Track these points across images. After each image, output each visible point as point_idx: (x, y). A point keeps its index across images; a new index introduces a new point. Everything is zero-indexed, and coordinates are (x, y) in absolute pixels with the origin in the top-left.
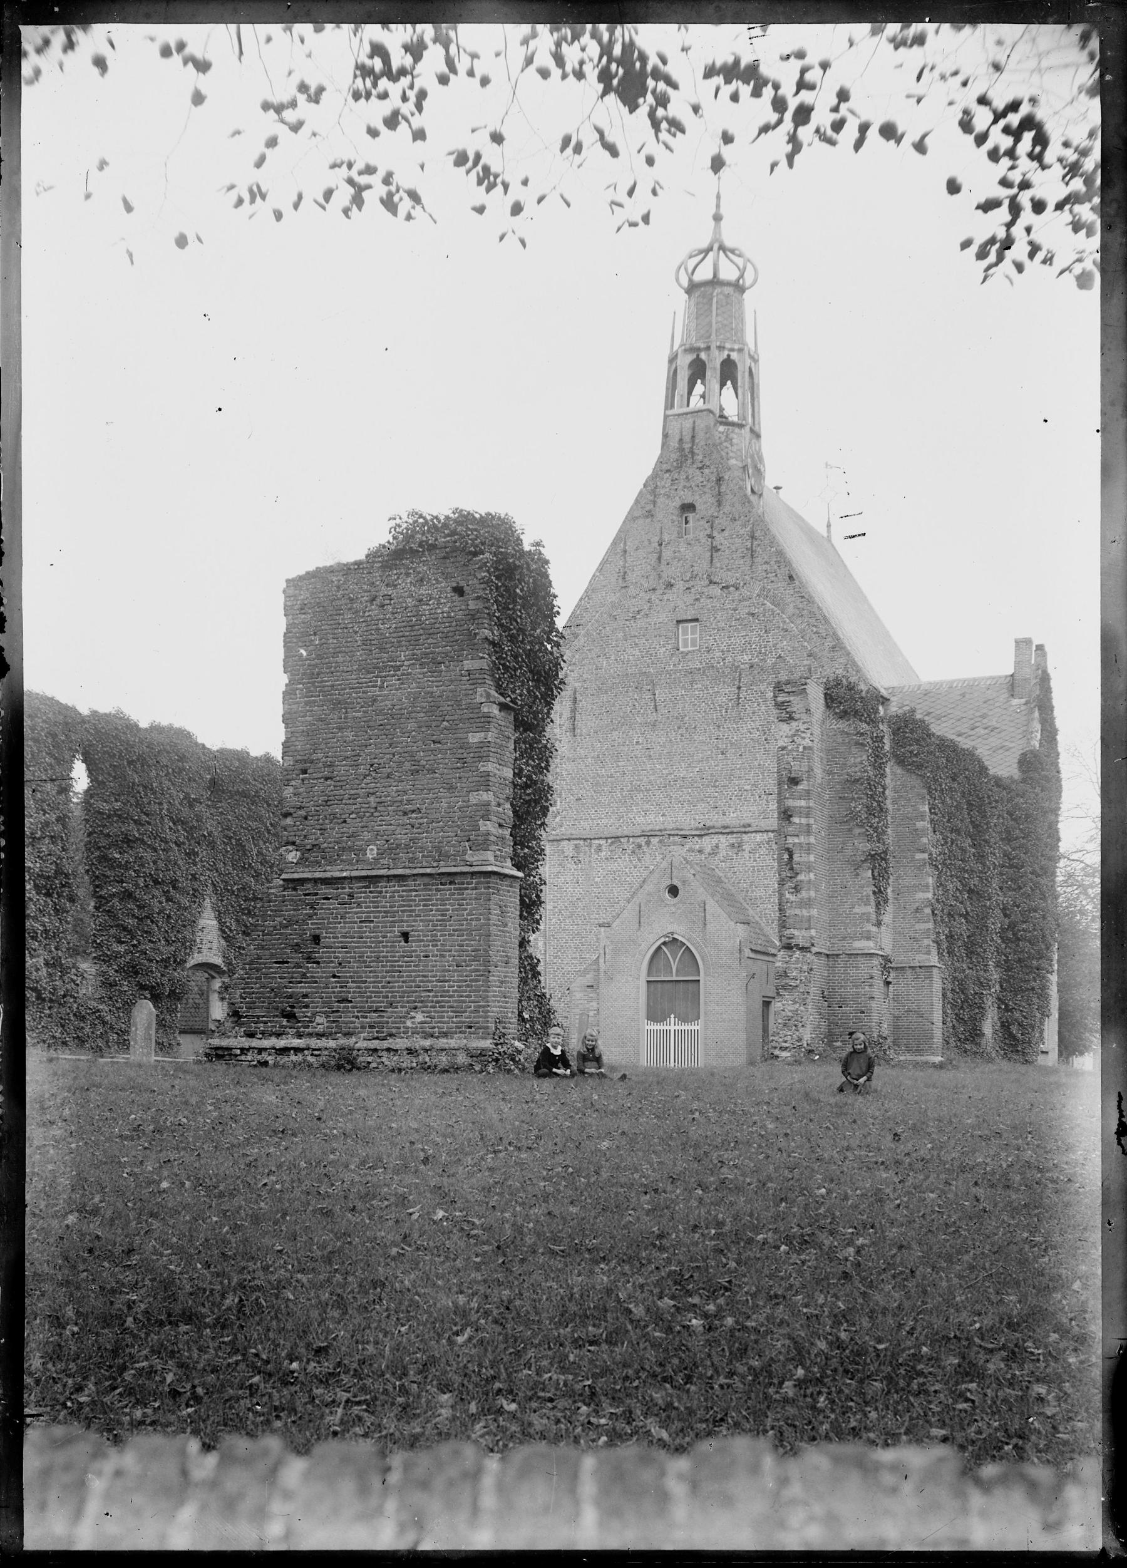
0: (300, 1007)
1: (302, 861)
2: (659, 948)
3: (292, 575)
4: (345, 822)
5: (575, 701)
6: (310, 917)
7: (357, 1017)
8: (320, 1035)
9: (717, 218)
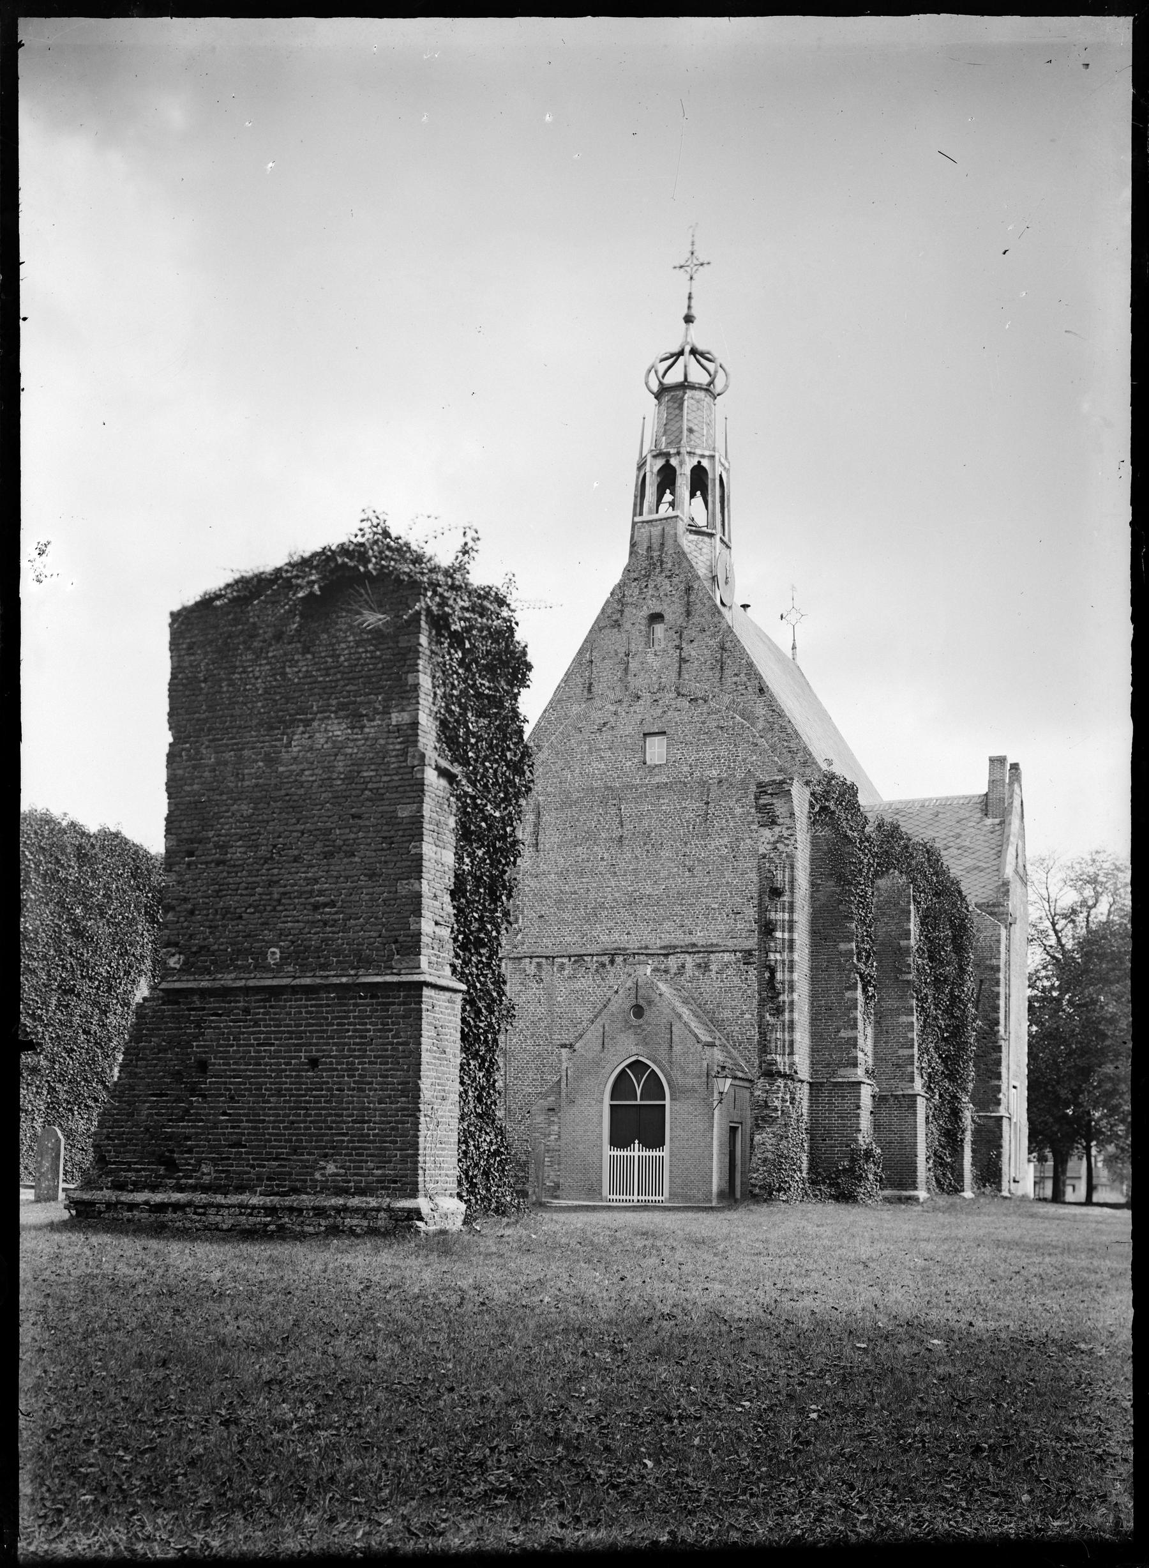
0: (182, 1153)
1: (186, 969)
2: (623, 1070)
3: (176, 607)
4: (240, 918)
5: (538, 815)
6: (196, 1038)
7: (253, 1167)
8: (205, 1189)
9: (688, 319)
